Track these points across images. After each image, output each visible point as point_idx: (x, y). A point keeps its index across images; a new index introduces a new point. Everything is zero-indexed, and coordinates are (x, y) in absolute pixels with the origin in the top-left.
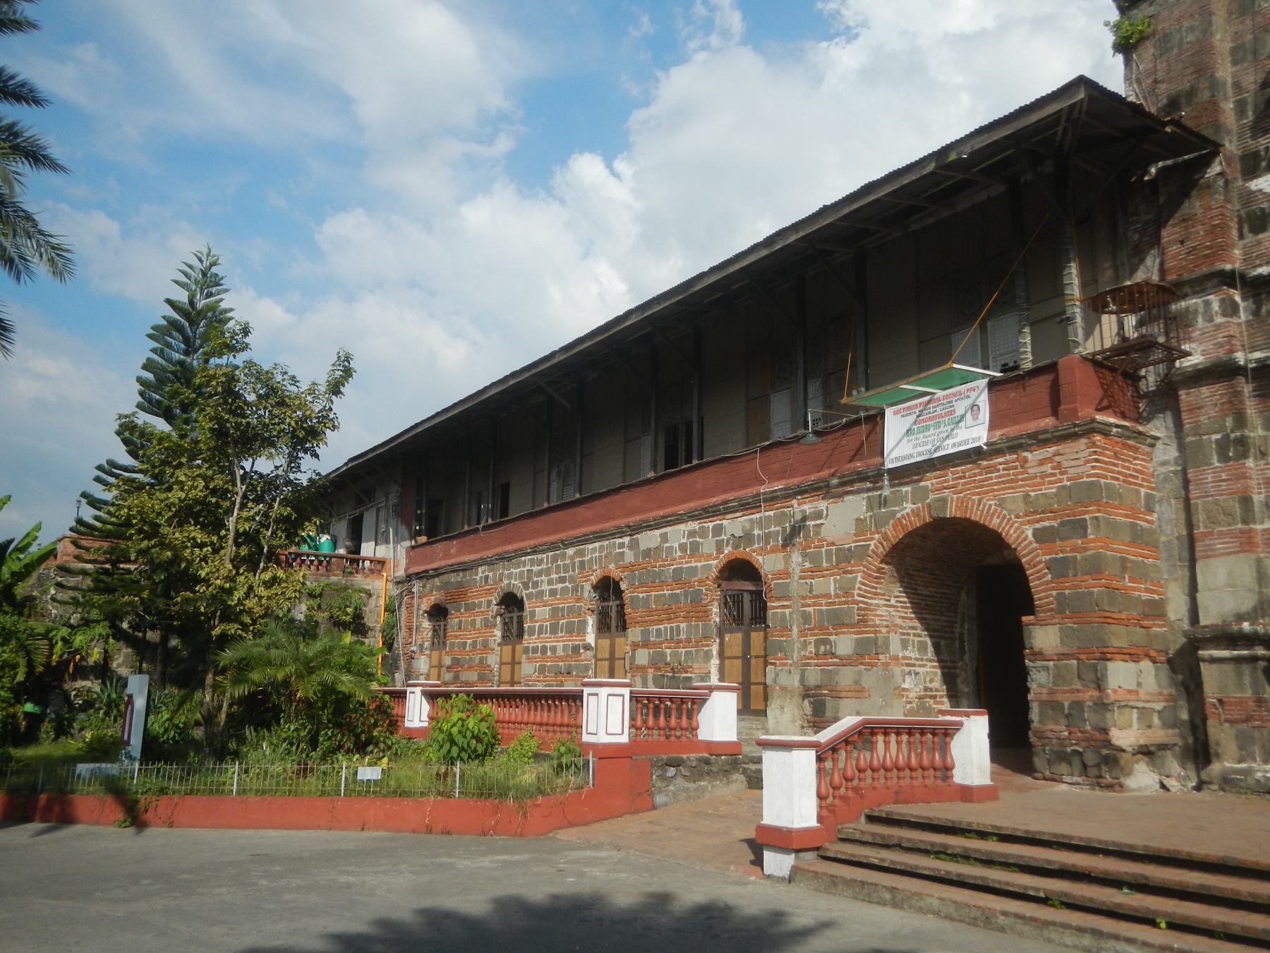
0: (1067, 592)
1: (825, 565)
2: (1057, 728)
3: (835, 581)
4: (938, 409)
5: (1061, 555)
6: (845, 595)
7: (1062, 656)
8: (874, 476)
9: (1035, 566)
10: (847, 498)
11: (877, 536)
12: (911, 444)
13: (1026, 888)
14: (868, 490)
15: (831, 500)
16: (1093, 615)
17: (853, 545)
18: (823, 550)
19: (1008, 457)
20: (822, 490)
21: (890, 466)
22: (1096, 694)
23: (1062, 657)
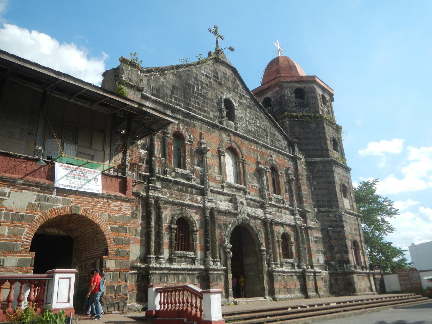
0: (119, 249)
1: (3, 219)
2: (112, 295)
3: (9, 229)
4: (81, 173)
5: (119, 237)
6: (15, 237)
7: (115, 271)
8: (44, 187)
9: (110, 239)
10: (24, 191)
11: (40, 213)
12: (68, 181)
13: (260, 321)
14: (39, 192)
15: (13, 189)
16: (126, 257)
17: (24, 214)
18: (3, 212)
19: (104, 200)
20: (11, 183)
21: (58, 186)
22: (125, 283)
23: (115, 271)
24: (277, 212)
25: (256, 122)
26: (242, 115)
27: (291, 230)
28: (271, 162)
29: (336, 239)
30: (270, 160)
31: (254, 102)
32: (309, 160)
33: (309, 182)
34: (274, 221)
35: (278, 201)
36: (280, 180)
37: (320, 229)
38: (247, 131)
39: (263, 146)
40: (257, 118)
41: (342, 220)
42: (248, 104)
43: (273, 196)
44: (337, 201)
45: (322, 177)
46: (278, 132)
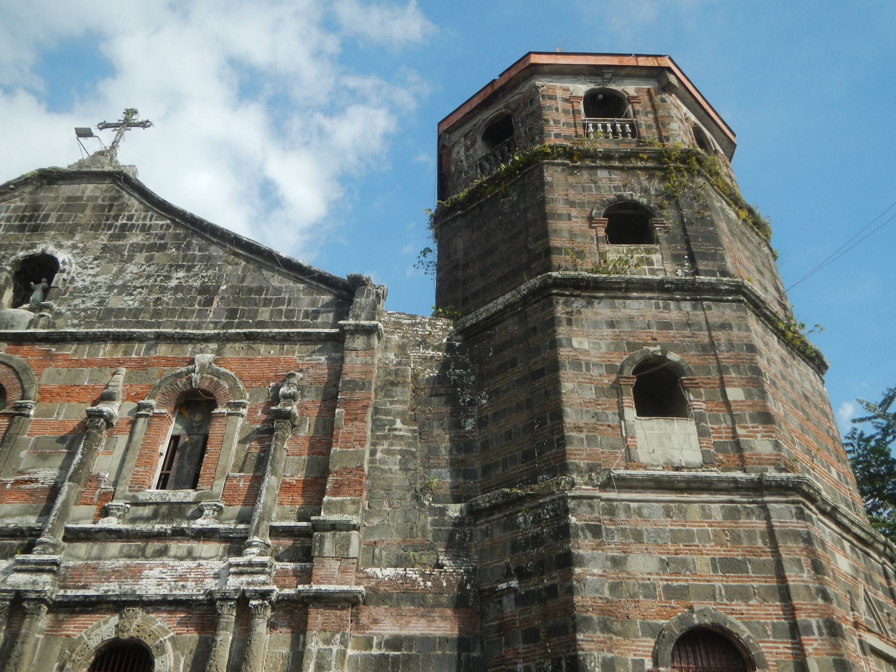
24: (130, 557)
25: (168, 278)
26: (97, 279)
27: (180, 623)
28: (181, 383)
29: (531, 636)
30: (179, 376)
31: (187, 228)
32: (470, 320)
33: (452, 399)
34: (34, 596)
35: (176, 510)
36: (215, 430)
37: (444, 599)
38: (98, 318)
39: (160, 338)
40: (179, 267)
41: (568, 525)
42: (152, 241)
43: (134, 496)
44: (562, 441)
45: (513, 363)
46: (288, 277)
